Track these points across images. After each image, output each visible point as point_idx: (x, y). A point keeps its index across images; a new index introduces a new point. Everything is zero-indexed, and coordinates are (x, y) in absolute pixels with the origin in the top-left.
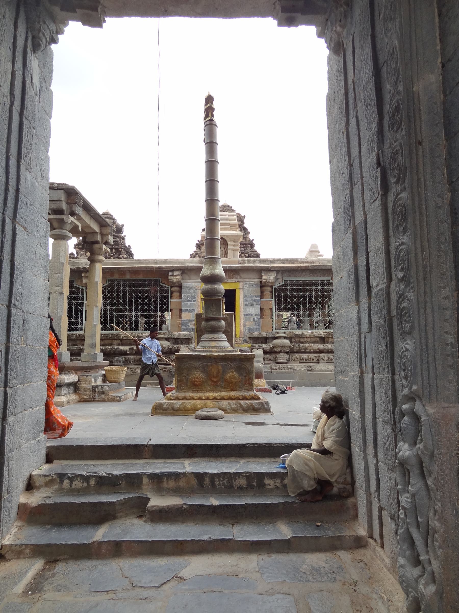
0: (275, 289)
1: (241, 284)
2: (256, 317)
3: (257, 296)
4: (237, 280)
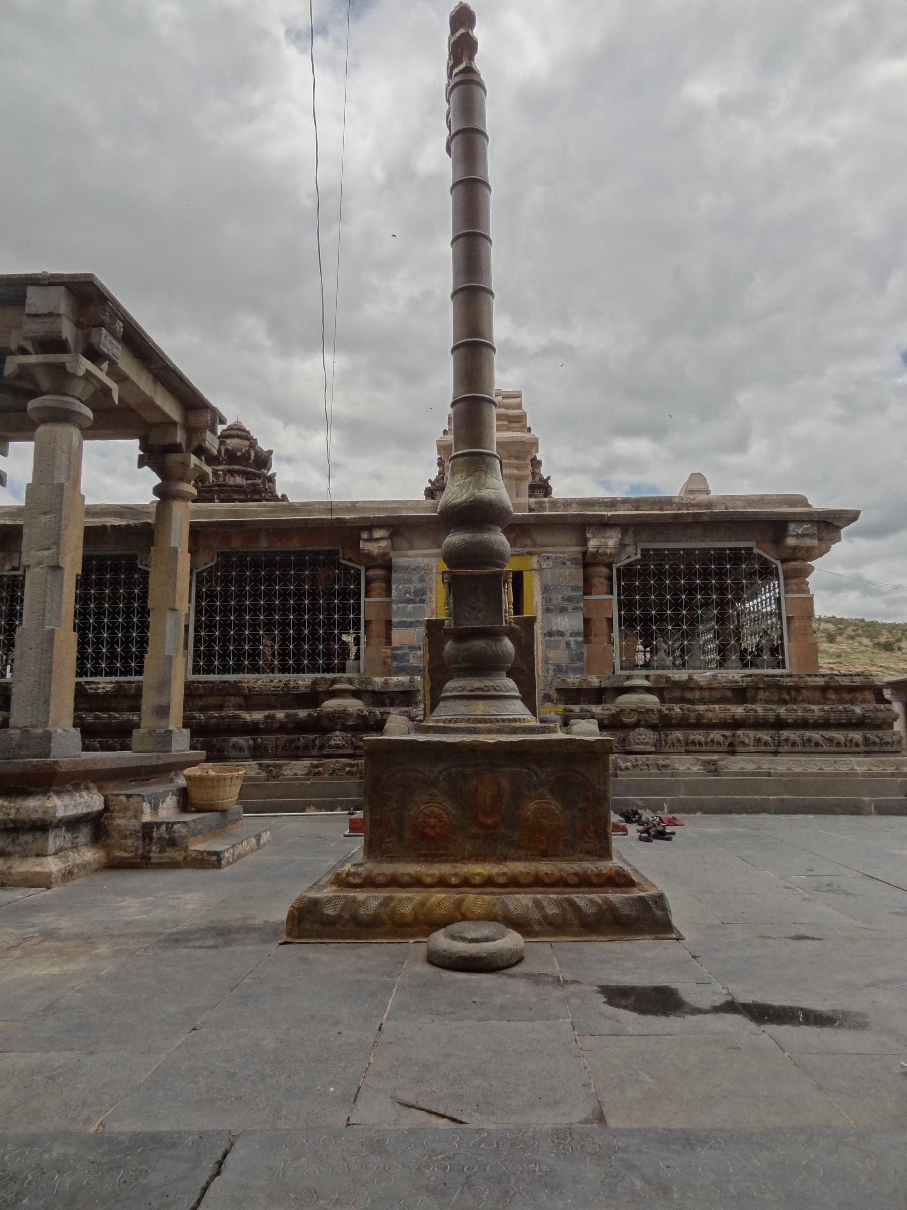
0: (618, 570)
1: (535, 559)
2: (572, 639)
3: (575, 589)
4: (526, 550)
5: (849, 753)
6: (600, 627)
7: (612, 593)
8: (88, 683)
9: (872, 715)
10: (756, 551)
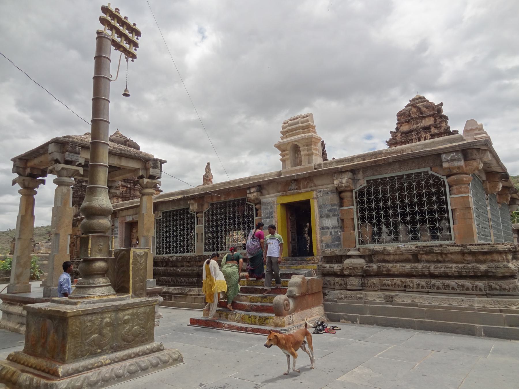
0: (356, 193)
1: (315, 193)
2: (333, 230)
3: (333, 205)
4: (310, 189)
5: (476, 295)
6: (348, 222)
7: (353, 205)
8: (171, 257)
9: (494, 270)
10: (430, 172)
